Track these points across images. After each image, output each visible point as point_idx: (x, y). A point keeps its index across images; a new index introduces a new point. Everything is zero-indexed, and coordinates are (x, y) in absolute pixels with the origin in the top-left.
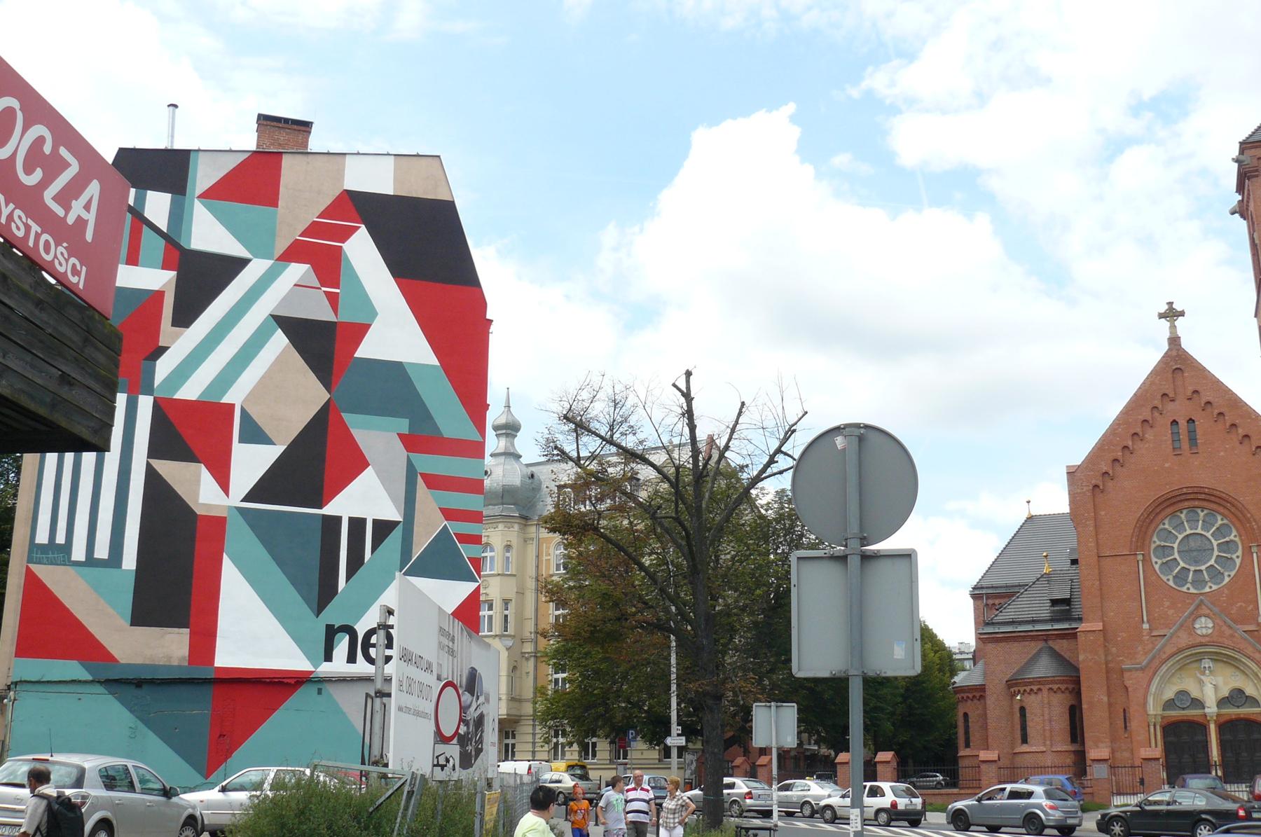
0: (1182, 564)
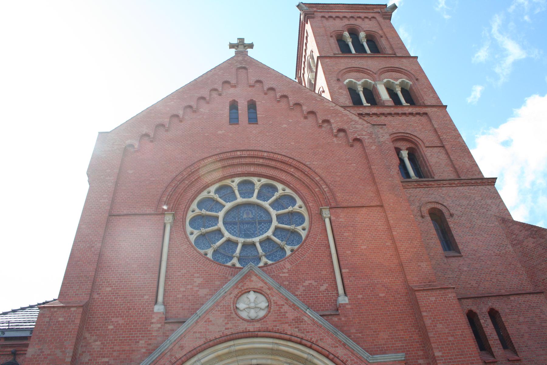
0: (227, 235)
